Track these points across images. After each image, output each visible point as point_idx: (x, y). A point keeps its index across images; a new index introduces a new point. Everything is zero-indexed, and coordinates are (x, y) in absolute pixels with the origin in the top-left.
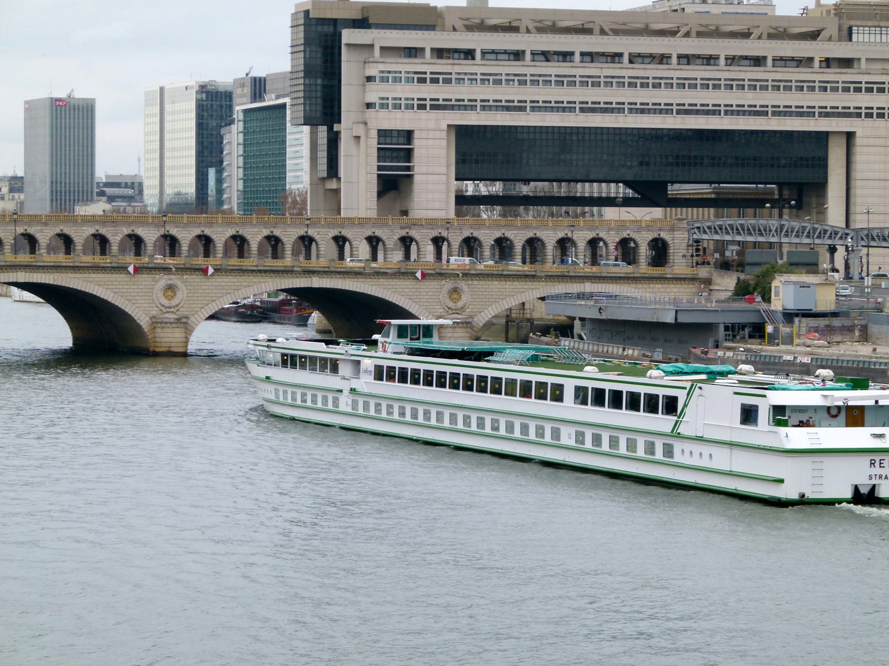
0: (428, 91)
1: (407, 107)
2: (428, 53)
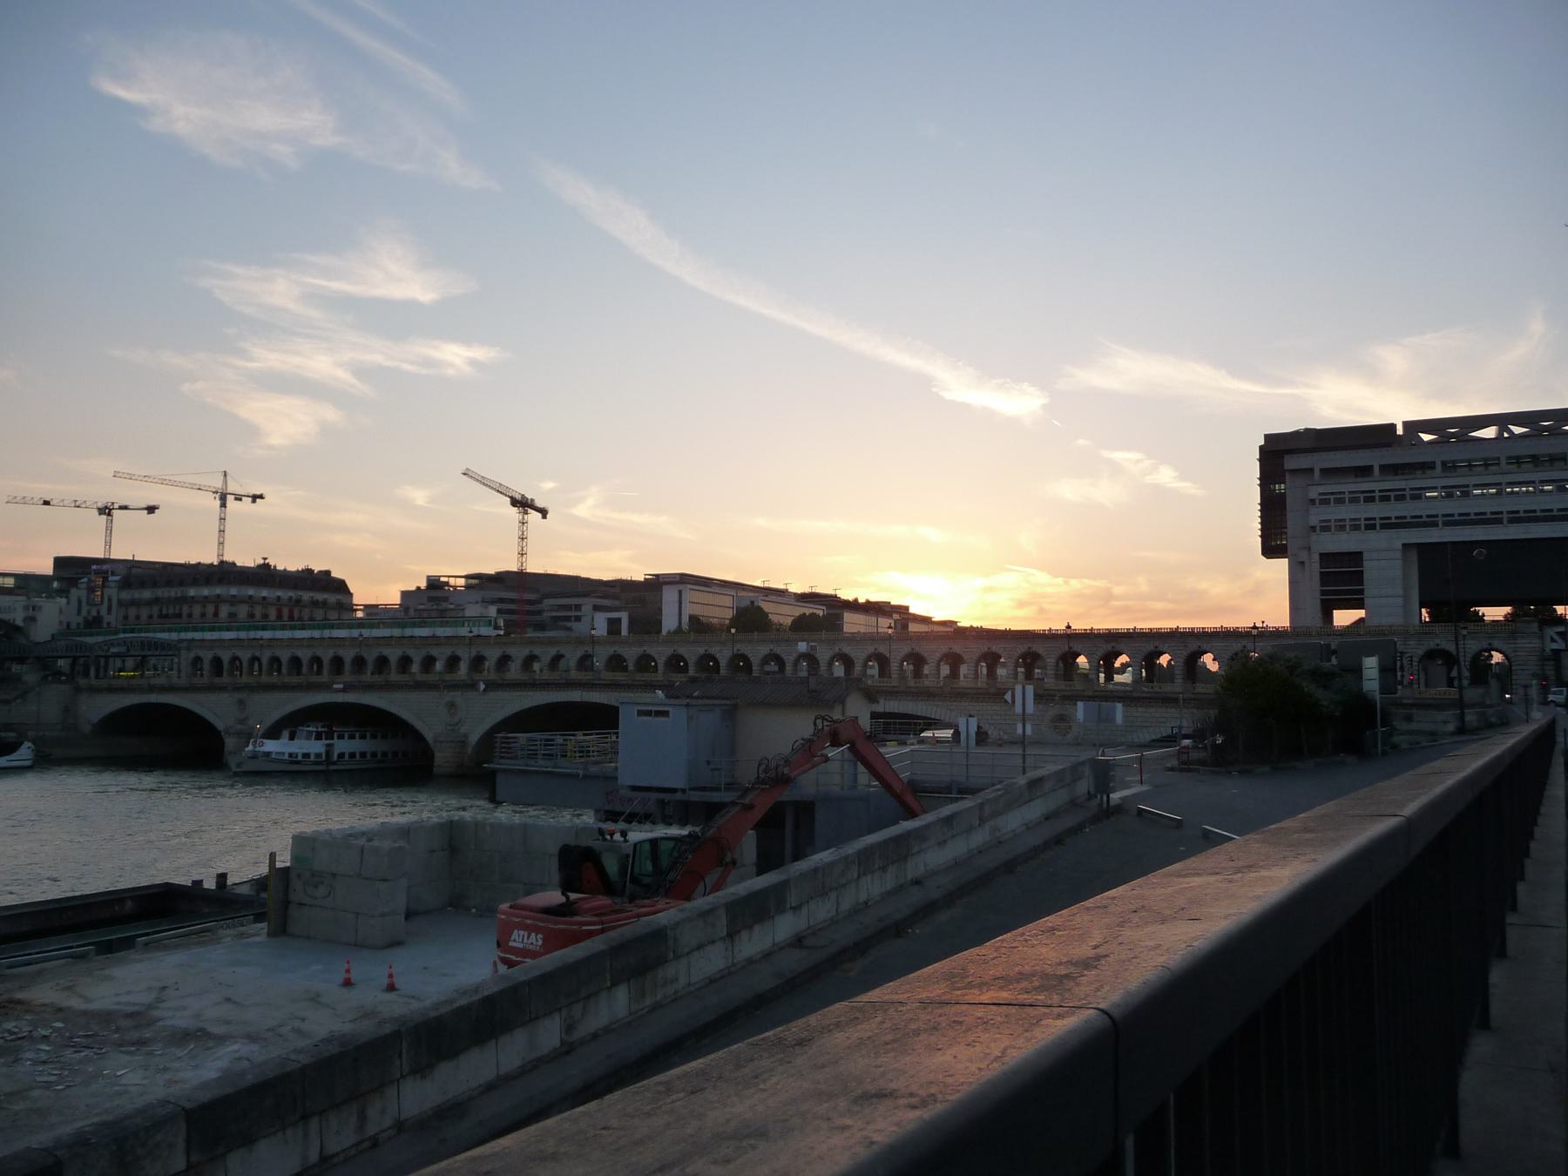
0: (1377, 510)
1: (1356, 528)
2: (1376, 470)
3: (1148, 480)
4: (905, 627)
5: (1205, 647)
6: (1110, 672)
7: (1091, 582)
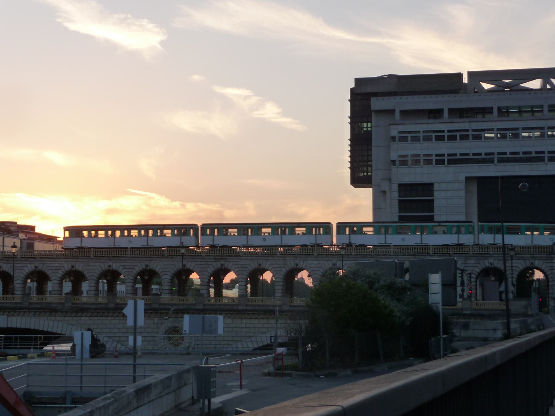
0: (446, 148)
1: (428, 162)
3: (256, 114)
4: (31, 246)
5: (301, 265)
6: (219, 287)
7: (202, 205)
